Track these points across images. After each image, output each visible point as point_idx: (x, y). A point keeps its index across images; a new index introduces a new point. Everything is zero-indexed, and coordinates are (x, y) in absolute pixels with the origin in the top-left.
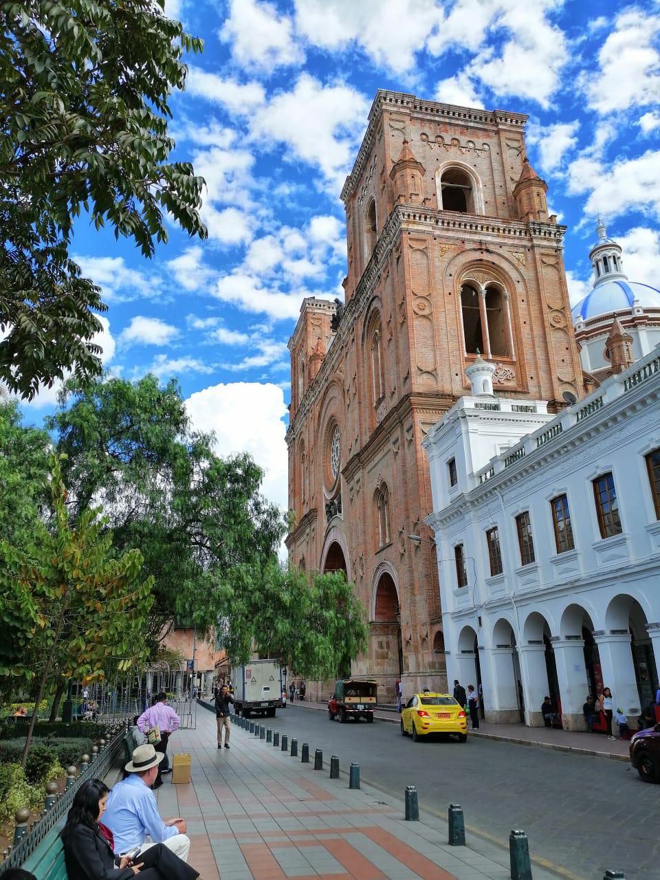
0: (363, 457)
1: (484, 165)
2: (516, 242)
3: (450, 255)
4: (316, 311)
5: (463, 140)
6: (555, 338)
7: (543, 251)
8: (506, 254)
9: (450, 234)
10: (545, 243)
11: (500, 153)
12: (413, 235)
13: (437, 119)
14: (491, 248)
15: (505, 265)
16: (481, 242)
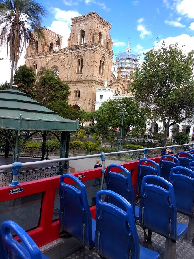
0: (72, 82)
1: (104, 34)
2: (108, 54)
3: (100, 55)
4: (46, 31)
5: (103, 27)
6: (109, 73)
7: (111, 57)
8: (106, 56)
9: (101, 50)
10: (111, 56)
11: (107, 32)
12: (97, 50)
13: (100, 21)
14: (105, 54)
15: (106, 58)
16: (104, 53)
